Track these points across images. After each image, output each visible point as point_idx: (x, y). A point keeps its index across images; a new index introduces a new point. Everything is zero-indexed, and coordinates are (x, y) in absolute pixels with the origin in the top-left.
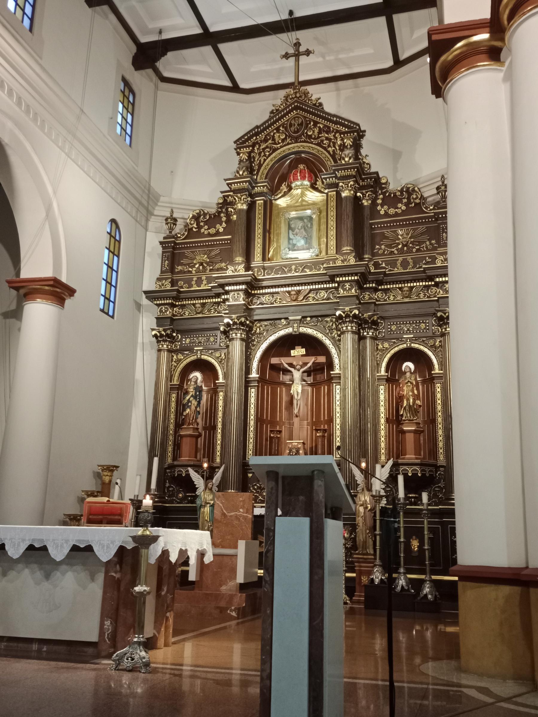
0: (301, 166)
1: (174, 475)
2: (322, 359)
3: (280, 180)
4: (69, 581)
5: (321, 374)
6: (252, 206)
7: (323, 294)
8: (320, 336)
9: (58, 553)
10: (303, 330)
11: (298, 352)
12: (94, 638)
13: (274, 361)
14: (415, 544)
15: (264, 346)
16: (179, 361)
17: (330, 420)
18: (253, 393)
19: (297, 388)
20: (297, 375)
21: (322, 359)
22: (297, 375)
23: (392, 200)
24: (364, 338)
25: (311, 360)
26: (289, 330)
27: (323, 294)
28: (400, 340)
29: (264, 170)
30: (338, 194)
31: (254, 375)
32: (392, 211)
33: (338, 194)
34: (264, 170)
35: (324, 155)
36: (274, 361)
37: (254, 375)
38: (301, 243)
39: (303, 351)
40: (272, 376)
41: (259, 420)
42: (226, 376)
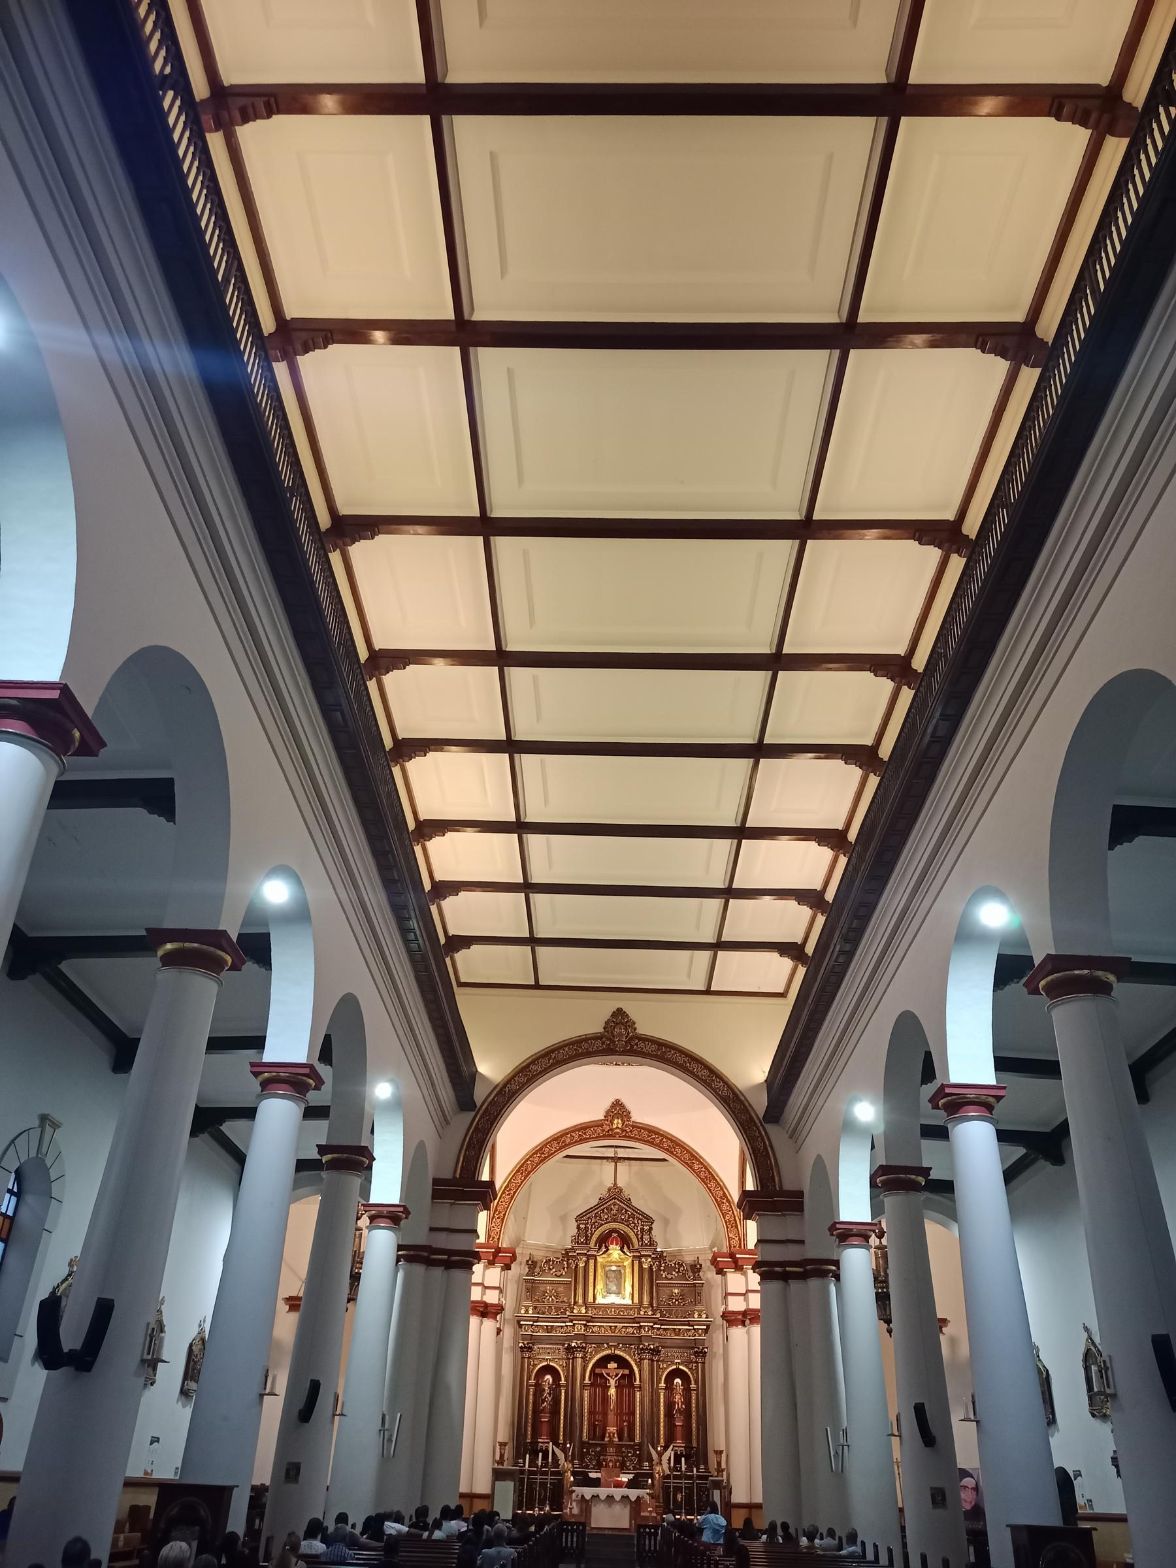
0: (615, 1235)
1: (699, 1481)
2: (627, 1372)
3: (604, 1241)
4: (617, 1508)
5: (627, 1382)
6: (587, 1263)
7: (631, 1330)
8: (627, 1357)
9: (618, 1498)
10: (617, 1352)
11: (612, 1365)
12: (627, 1526)
13: (598, 1371)
14: (679, 1497)
15: (593, 1361)
16: (535, 1365)
17: (633, 1413)
18: (586, 1393)
19: (612, 1391)
20: (612, 1382)
21: (627, 1372)
22: (612, 1382)
23: (668, 1269)
24: (652, 1361)
25: (621, 1372)
26: (608, 1352)
27: (631, 1330)
28: (673, 1363)
29: (594, 1238)
30: (640, 1264)
31: (587, 1381)
32: (669, 1276)
33: (640, 1264)
34: (594, 1238)
35: (631, 1234)
36: (598, 1371)
37: (587, 1381)
38: (614, 1288)
39: (615, 1365)
40: (599, 1382)
41: (590, 1412)
42: (566, 1379)
